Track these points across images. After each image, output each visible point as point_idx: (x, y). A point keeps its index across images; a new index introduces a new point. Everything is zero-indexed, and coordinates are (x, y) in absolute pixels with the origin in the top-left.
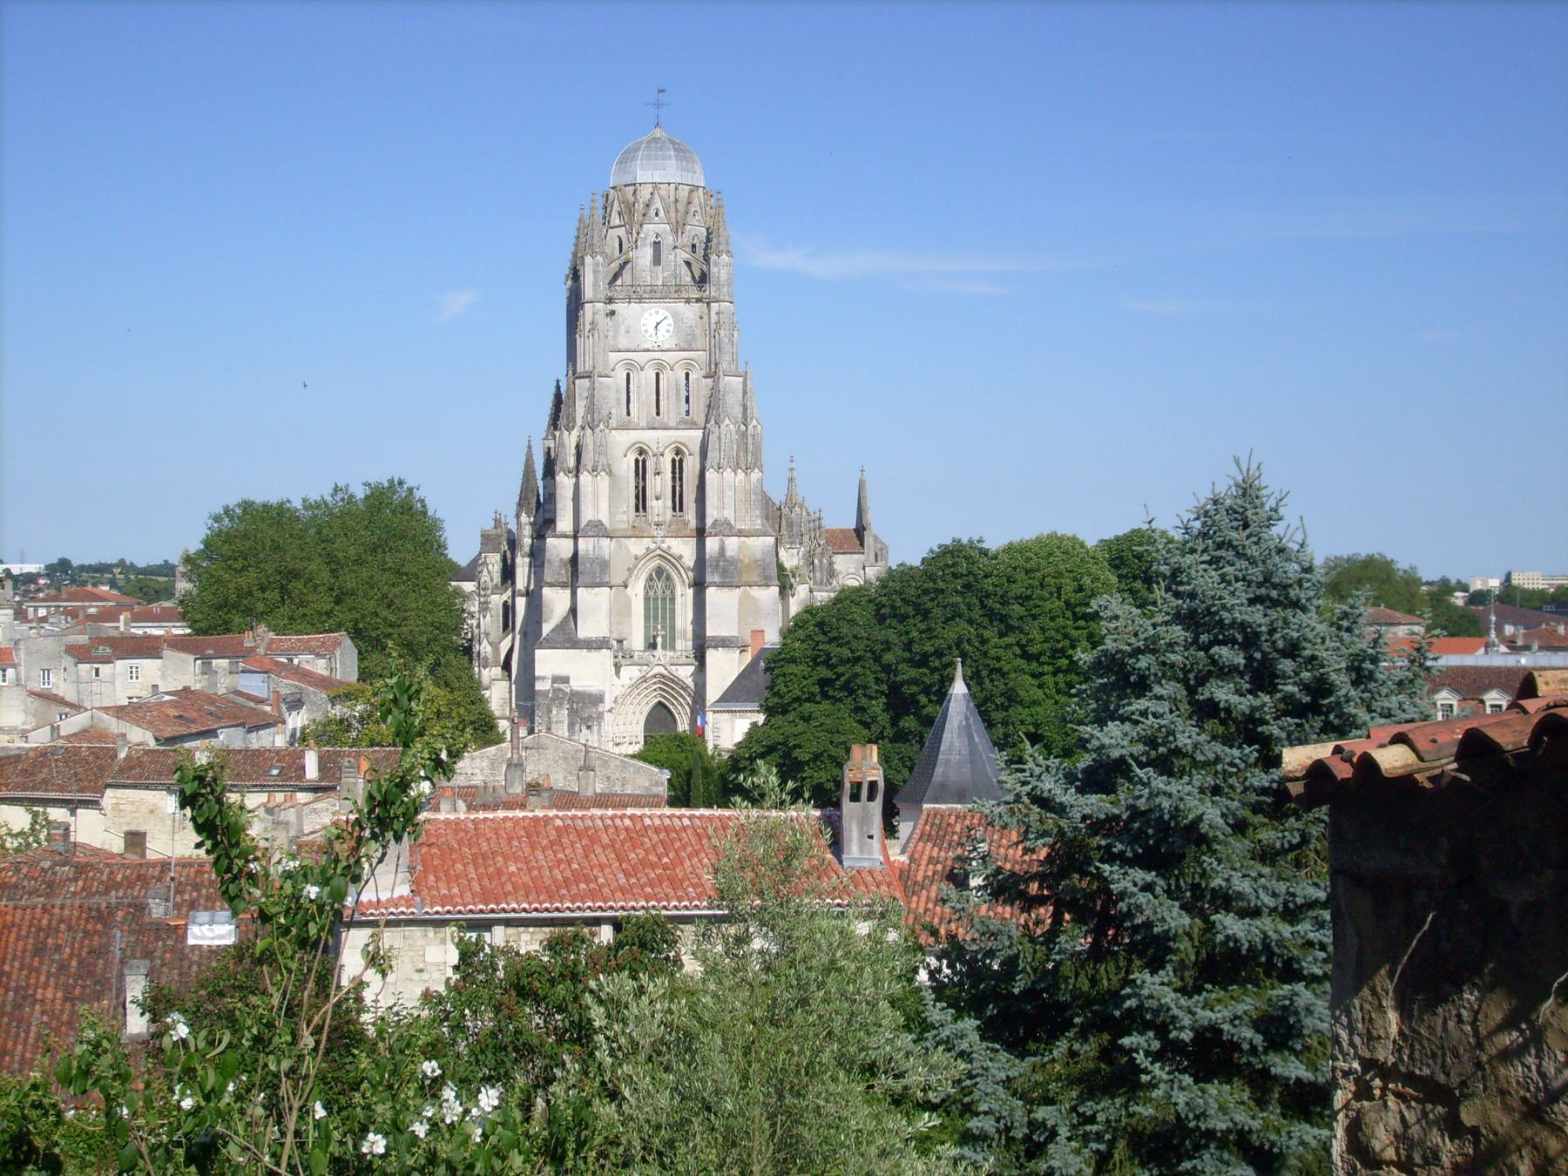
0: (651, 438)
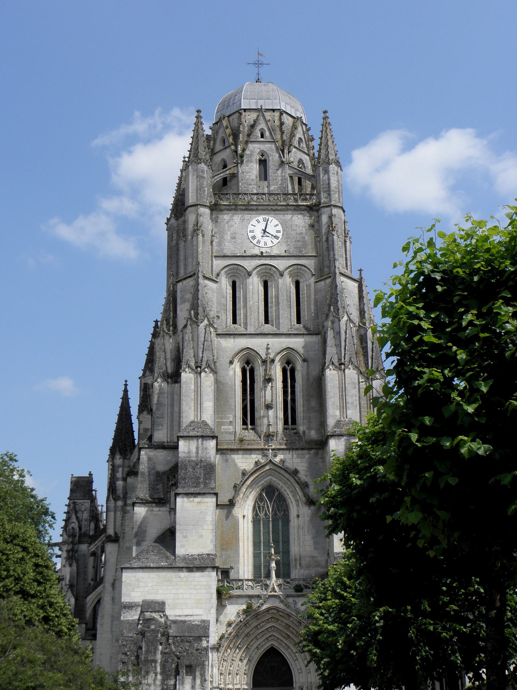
0: (258, 344)
